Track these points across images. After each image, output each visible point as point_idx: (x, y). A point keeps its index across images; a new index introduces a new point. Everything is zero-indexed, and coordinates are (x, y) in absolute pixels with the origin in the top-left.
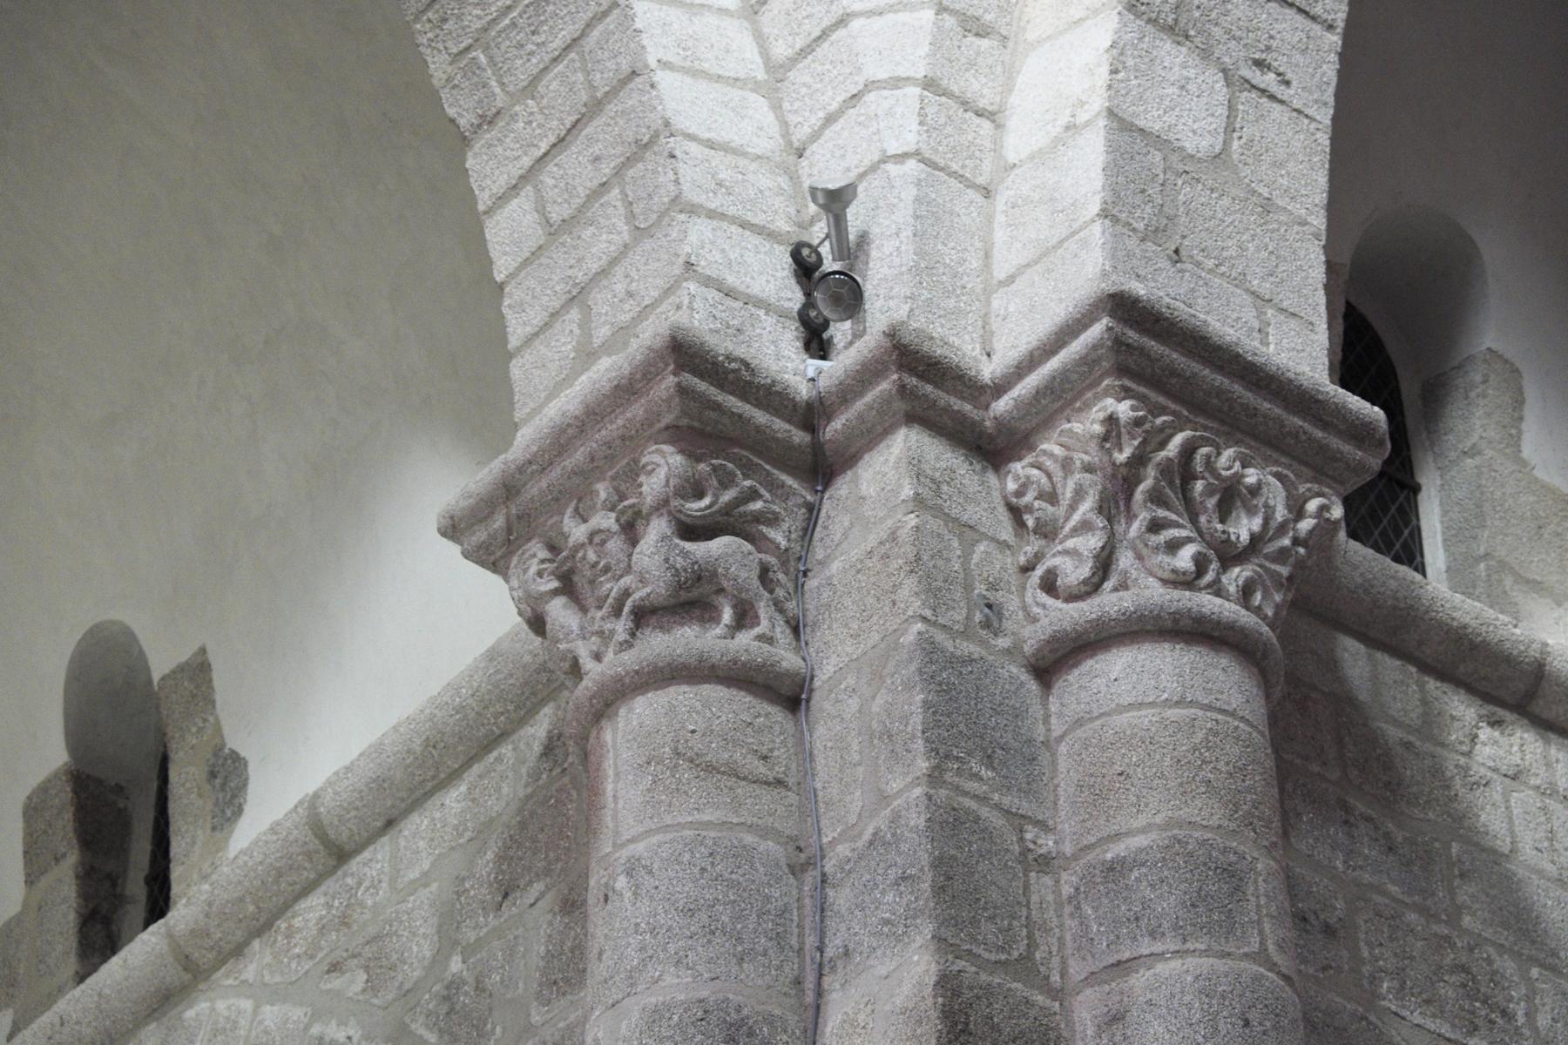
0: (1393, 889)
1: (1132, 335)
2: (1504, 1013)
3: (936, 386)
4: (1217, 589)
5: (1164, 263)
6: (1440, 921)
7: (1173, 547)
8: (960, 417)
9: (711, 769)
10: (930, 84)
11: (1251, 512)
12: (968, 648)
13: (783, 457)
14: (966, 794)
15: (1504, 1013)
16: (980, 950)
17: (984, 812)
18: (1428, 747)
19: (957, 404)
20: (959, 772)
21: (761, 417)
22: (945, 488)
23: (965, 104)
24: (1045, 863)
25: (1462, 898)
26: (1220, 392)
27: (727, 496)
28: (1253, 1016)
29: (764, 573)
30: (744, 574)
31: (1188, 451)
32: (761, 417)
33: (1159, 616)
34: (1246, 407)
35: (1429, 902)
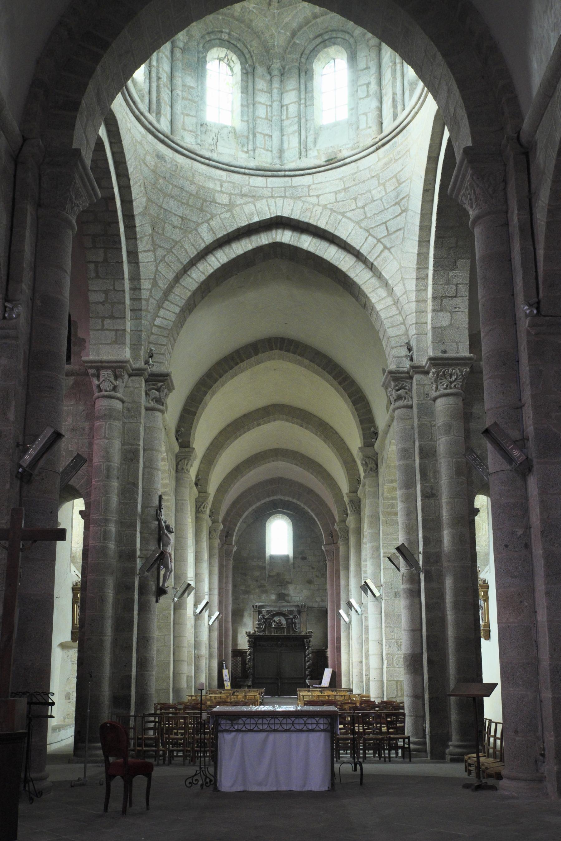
1: (433, 362)
4: (451, 388)
7: (443, 385)
10: (416, 323)
12: (424, 402)
13: (406, 378)
17: (426, 422)
21: (402, 375)
23: (422, 324)
24: (434, 426)
29: (406, 393)
31: (444, 372)
32: (402, 375)
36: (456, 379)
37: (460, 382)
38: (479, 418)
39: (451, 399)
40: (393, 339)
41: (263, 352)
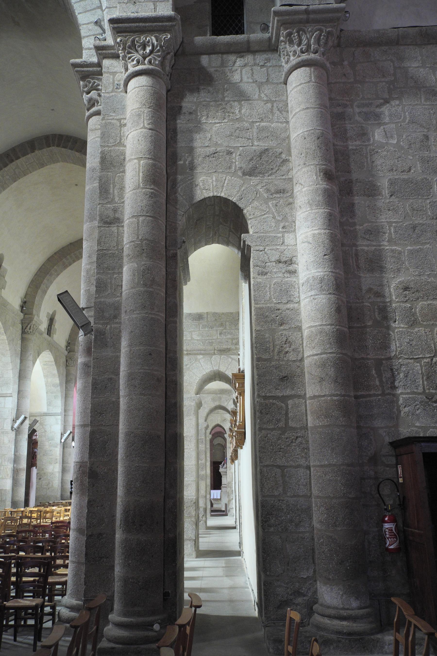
0: (208, 100)
1: (116, 25)
2: (233, 113)
3: (106, 50)
5: (132, 6)
6: (218, 101)
8: (112, 54)
9: (93, 130)
11: (149, 46)
12: (111, 94)
14: (109, 119)
15: (233, 113)
16: (110, 145)
17: (113, 121)
18: (222, 68)
19: (110, 51)
20: (108, 117)
21: (91, 69)
22: (110, 67)
25: (226, 94)
26: (137, 27)
27: (91, 85)
28: (140, 139)
30: (95, 96)
31: (133, 41)
32: (91, 69)
33: (130, 75)
34: (143, 27)
35: (217, 99)
36: (151, 52)
37: (159, 56)
38: (190, 113)
39: (143, 80)
40: (84, 26)
41: (40, 149)
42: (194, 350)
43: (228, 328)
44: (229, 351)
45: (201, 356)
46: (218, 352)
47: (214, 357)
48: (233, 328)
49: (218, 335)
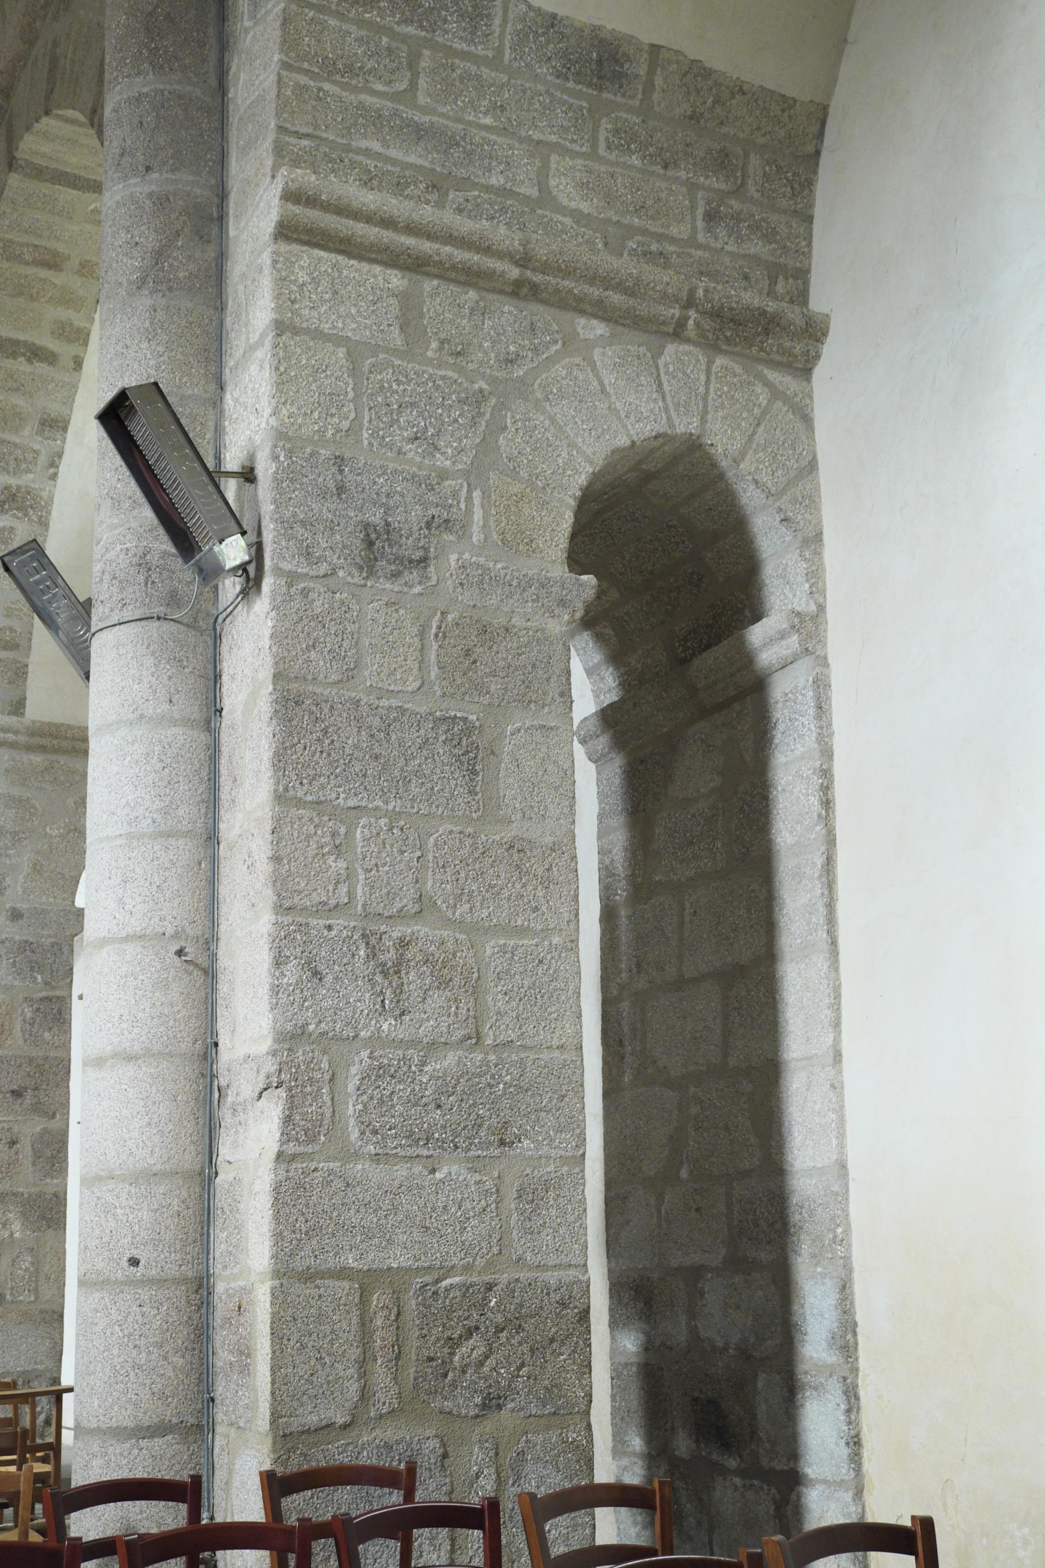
42: (568, 272)
43: (752, 189)
44: (767, 332)
45: (600, 329)
46: (707, 324)
47: (671, 349)
48: (784, 203)
49: (700, 224)
